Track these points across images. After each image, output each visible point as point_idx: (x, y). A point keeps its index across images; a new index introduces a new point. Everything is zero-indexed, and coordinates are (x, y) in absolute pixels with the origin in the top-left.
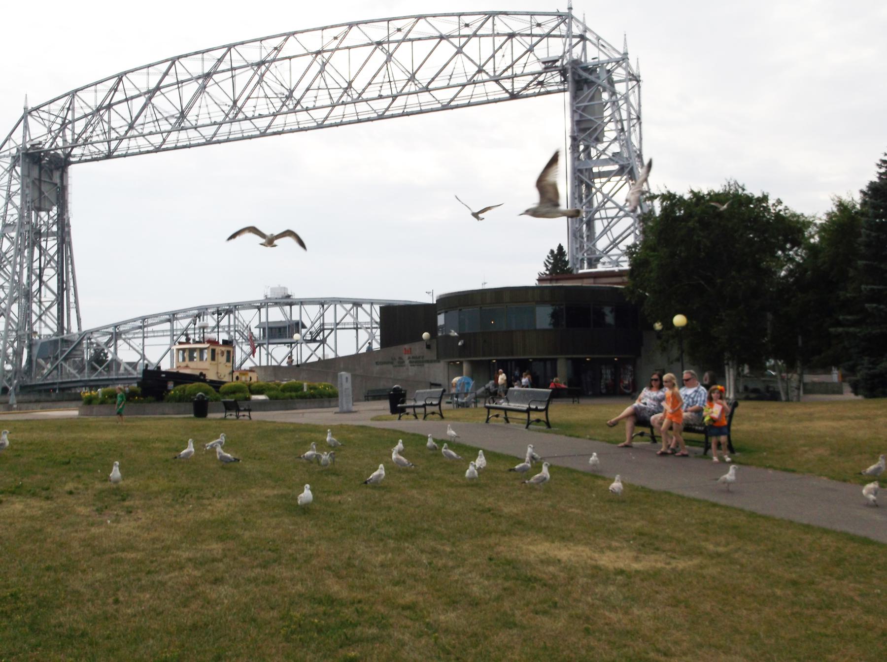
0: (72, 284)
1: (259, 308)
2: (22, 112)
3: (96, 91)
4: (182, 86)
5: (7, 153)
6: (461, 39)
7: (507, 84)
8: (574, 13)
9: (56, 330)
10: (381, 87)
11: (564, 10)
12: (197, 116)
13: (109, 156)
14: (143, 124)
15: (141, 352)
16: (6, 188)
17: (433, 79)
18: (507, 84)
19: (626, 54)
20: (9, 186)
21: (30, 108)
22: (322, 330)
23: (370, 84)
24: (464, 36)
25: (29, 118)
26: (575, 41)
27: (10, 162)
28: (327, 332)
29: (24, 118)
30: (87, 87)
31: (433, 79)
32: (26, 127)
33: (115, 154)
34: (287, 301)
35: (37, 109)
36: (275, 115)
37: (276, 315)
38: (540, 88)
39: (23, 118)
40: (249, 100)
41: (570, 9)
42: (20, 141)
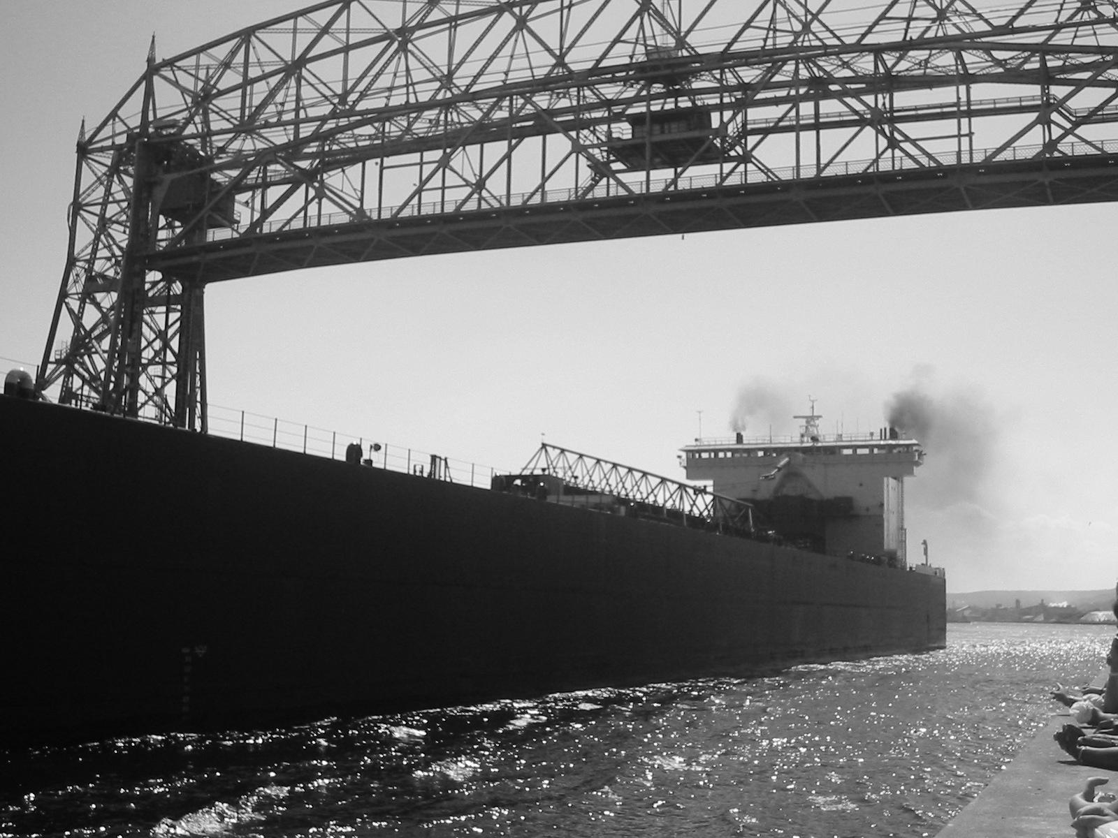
0: (199, 398)
3: (295, 31)
4: (455, 27)
5: (109, 143)
12: (506, 74)
14: (390, 89)
16: (97, 209)
17: (1022, 12)
21: (158, 60)
23: (883, 17)
25: (156, 78)
27: (109, 162)
29: (147, 77)
32: (149, 94)
35: (170, 63)
39: (144, 77)
40: (618, 46)
42: (135, 122)
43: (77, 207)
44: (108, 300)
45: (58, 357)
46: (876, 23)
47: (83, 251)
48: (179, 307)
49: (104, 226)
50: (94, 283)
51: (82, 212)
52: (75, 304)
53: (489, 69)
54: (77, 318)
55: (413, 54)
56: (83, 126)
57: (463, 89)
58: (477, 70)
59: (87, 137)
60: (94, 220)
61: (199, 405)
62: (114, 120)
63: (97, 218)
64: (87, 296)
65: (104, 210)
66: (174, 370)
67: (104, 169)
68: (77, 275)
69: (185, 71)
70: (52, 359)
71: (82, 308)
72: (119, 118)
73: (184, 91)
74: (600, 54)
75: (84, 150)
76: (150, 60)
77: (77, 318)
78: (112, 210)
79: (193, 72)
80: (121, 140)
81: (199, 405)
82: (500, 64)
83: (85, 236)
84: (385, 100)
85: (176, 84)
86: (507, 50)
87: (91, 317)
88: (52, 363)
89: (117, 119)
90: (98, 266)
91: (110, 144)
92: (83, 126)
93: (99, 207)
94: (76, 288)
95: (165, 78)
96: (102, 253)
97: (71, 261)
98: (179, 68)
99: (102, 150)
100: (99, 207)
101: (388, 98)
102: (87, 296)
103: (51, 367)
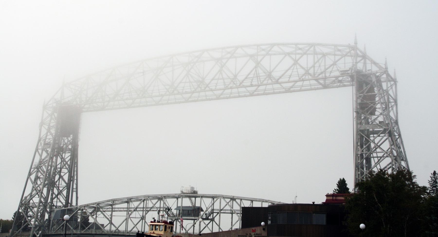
0: (75, 178)
1: (177, 198)
7: (322, 82)
9: (64, 204)
10: (252, 80)
11: (352, 44)
15: (110, 219)
17: (280, 77)
18: (322, 82)
20: (50, 124)
22: (212, 212)
23: (246, 78)
24: (299, 54)
26: (359, 59)
28: (215, 214)
31: (280, 77)
34: (193, 194)
36: (193, 92)
37: (187, 203)
41: (356, 43)
45: (34, 167)
46: (244, 80)
47: (43, 136)
51: (44, 125)
52: (40, 151)
54: (41, 156)
61: (75, 180)
70: (33, 167)
71: (42, 153)
77: (41, 156)
81: (75, 180)
83: (44, 132)
88: (33, 168)
103: (32, 170)
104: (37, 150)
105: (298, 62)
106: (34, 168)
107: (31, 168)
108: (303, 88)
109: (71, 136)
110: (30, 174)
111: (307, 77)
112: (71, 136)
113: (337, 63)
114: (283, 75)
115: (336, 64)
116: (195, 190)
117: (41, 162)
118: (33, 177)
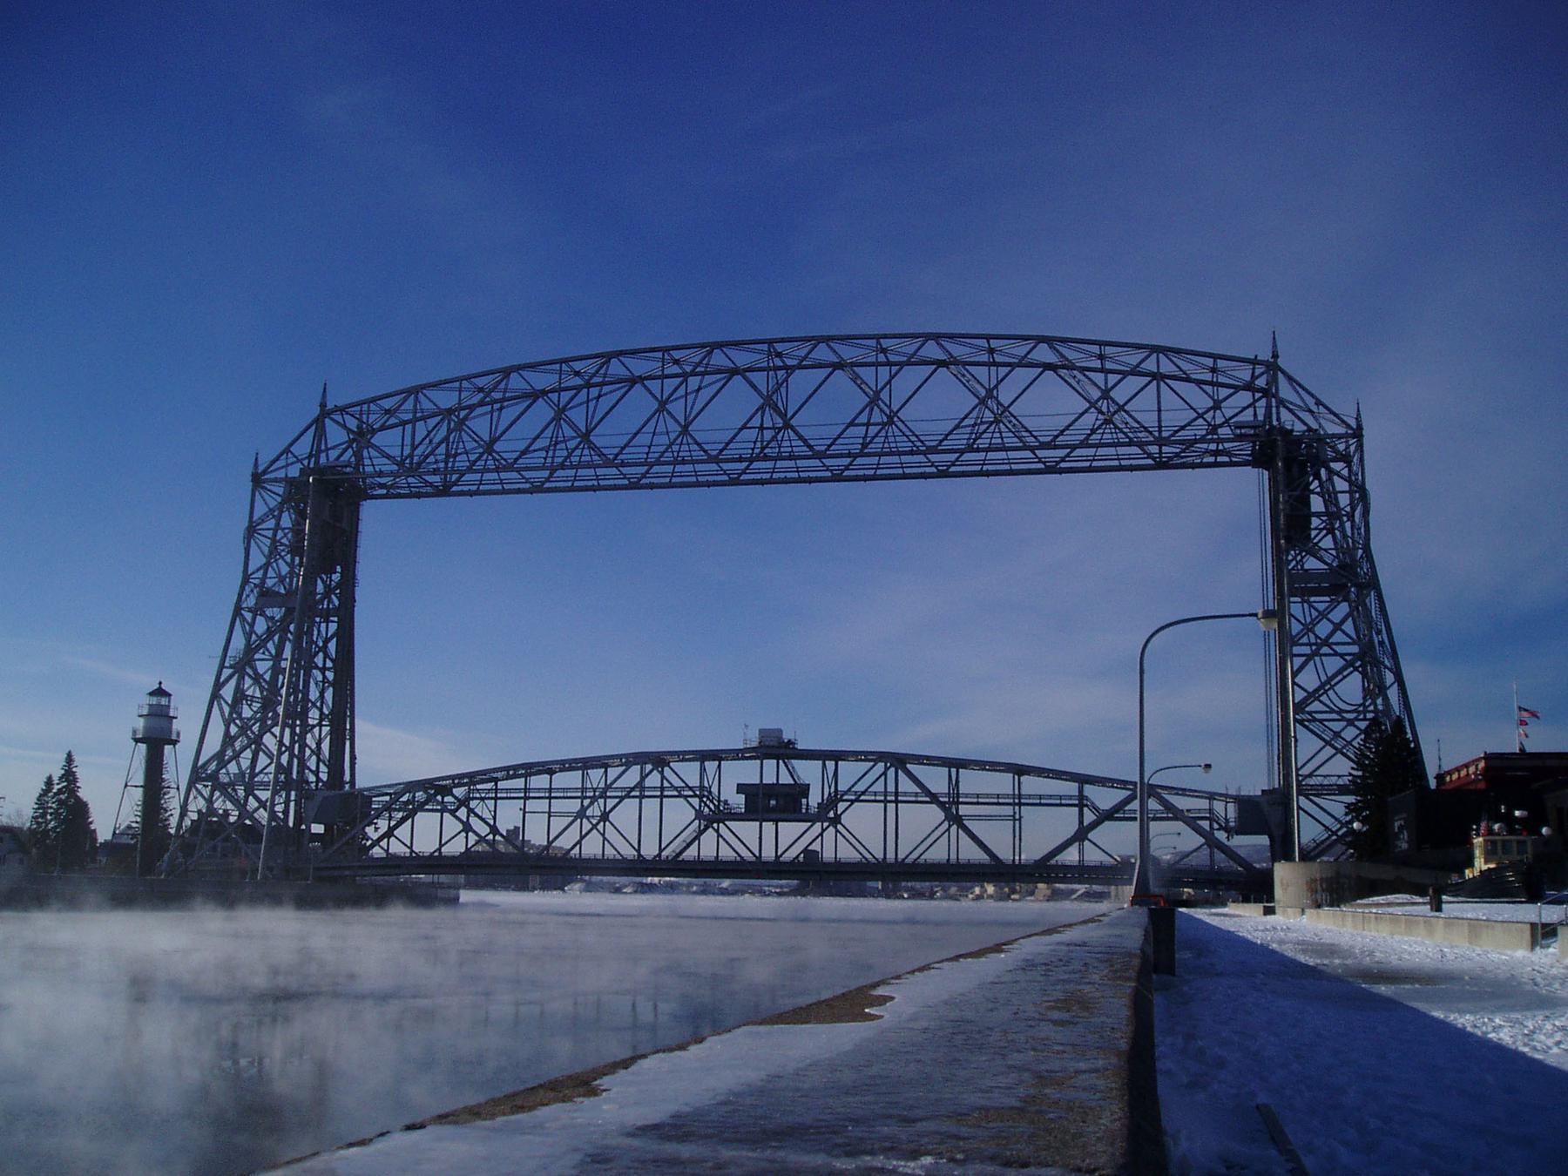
2: (317, 411)
5: (281, 474)
6: (1110, 376)
7: (1154, 449)
8: (1280, 362)
11: (1265, 355)
13: (444, 491)
15: (492, 822)
16: (270, 534)
18: (1154, 449)
19: (1360, 427)
21: (330, 406)
23: (957, 427)
26: (1258, 395)
27: (280, 491)
28: (841, 806)
29: (319, 423)
30: (446, 382)
32: (321, 434)
33: (455, 489)
35: (342, 410)
37: (771, 773)
38: (1220, 459)
39: (316, 421)
41: (1275, 356)
43: (251, 531)
44: (277, 613)
46: (951, 433)
48: (336, 619)
49: (276, 548)
50: (266, 596)
52: (248, 616)
53: (631, 444)
55: (565, 420)
56: (256, 459)
57: (611, 457)
58: (625, 442)
59: (261, 469)
60: (268, 542)
62: (287, 455)
63: (269, 541)
64: (257, 611)
65: (275, 535)
66: (330, 675)
67: (279, 499)
68: (252, 591)
69: (352, 415)
70: (227, 664)
71: (254, 619)
72: (292, 453)
73: (349, 431)
74: (729, 438)
75: (258, 480)
76: (323, 405)
78: (280, 534)
79: (358, 416)
80: (294, 472)
82: (643, 439)
83: (257, 560)
84: (543, 461)
85: (344, 426)
86: (650, 428)
87: (261, 626)
88: (227, 667)
89: (290, 455)
90: (269, 583)
91: (283, 476)
92: (256, 459)
93: (271, 531)
94: (251, 602)
95: (333, 419)
96: (271, 573)
97: (246, 579)
98: (347, 413)
99: (276, 480)
100: (271, 531)
101: (545, 459)
102: (257, 611)
103: (226, 672)
104: (238, 611)
105: (1112, 394)
106: (231, 667)
107: (222, 667)
108: (1095, 464)
109: (339, 569)
110: (218, 685)
111: (1108, 438)
112: (339, 569)
113: (1223, 405)
114: (1067, 428)
115: (1220, 408)
116: (786, 736)
117: (250, 651)
118: (228, 692)
